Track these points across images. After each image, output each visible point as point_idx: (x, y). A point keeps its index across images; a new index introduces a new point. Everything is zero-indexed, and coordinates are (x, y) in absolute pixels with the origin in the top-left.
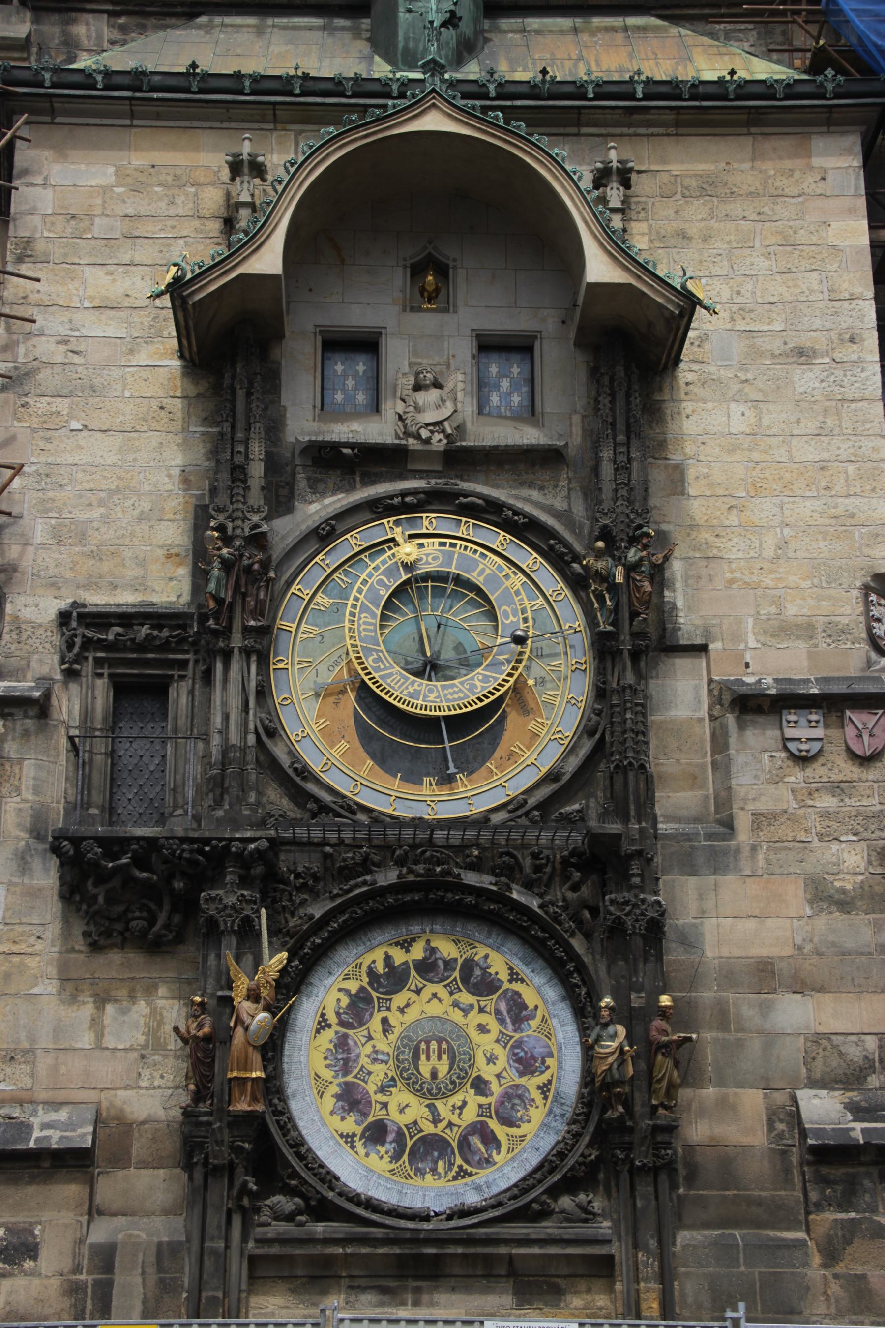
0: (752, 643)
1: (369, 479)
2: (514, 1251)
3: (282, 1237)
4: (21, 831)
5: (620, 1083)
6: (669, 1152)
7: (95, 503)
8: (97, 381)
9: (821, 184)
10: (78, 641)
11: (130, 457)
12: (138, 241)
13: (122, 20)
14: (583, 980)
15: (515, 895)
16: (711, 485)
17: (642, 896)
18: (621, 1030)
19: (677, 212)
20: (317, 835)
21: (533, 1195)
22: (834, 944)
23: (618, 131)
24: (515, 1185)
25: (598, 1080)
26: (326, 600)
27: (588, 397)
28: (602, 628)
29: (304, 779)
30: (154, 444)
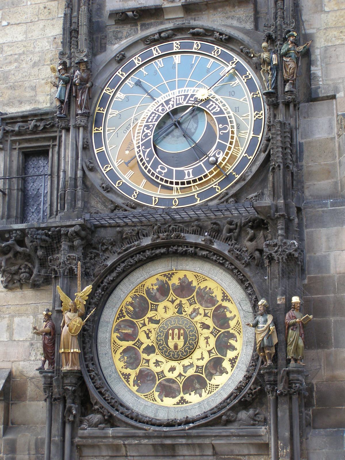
1: (144, 27)
2: (213, 442)
3: (91, 435)
6: (298, 385)
15: (215, 246)
17: (285, 241)
21: (223, 411)
24: (216, 407)
26: (122, 95)
29: (108, 192)
30: (41, 26)
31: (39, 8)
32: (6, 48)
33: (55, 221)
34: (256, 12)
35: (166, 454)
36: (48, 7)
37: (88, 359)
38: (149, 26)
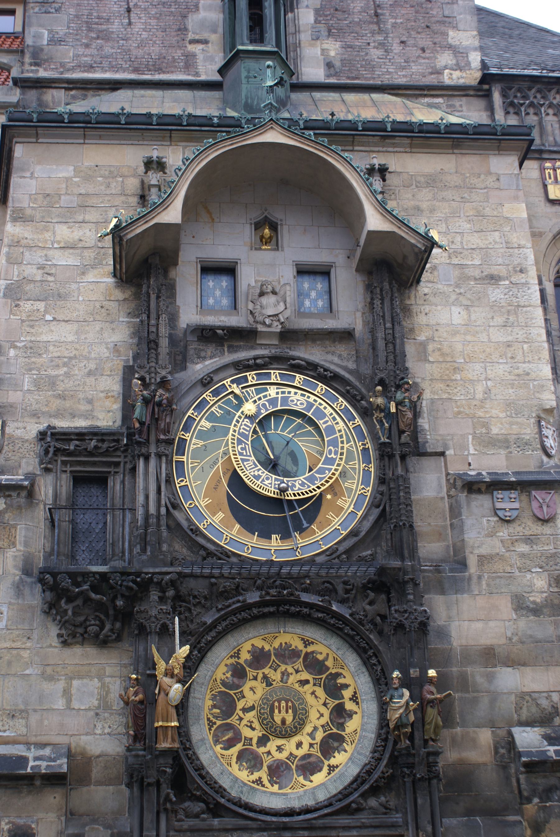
0: (472, 451)
1: (232, 349)
2: (340, 834)
4: (17, 570)
5: (404, 726)
7: (61, 365)
8: (62, 291)
9: (497, 183)
10: (51, 450)
11: (83, 337)
12: (88, 209)
13: (73, 92)
14: (378, 661)
15: (334, 608)
16: (443, 355)
17: (415, 607)
18: (407, 693)
19: (413, 196)
20: (207, 571)
21: (352, 798)
22: (531, 636)
23: (376, 149)
24: (340, 793)
25: (392, 725)
26: (208, 423)
28: (382, 440)
29: (197, 535)
30: (98, 328)
31: (95, 307)
32: (51, 348)
34: (356, 353)
37: (183, 734)
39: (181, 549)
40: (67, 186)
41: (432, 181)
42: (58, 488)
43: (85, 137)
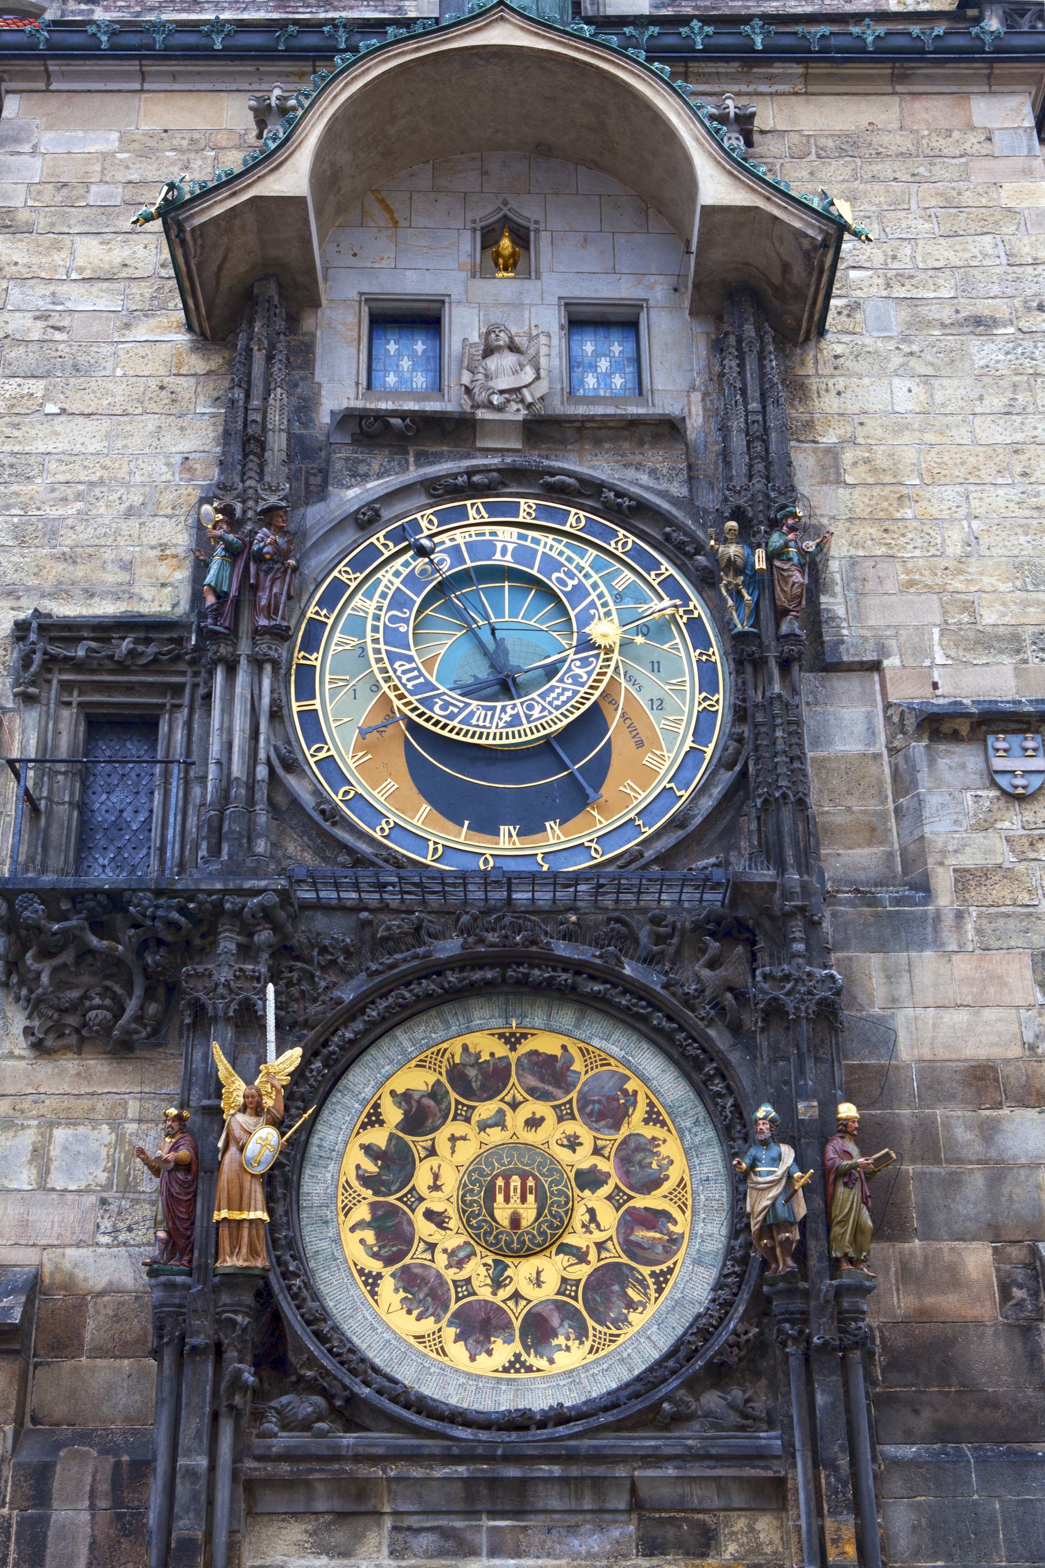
0: (940, 659)
2: (636, 1473)
7: (71, 497)
8: (82, 359)
9: (987, 145)
10: (37, 658)
11: (119, 444)
14: (728, 1087)
15: (628, 971)
16: (874, 471)
17: (808, 969)
19: (812, 174)
24: (638, 1379)
27: (710, 372)
29: (334, 824)
30: (151, 427)
32: (53, 466)
33: (207, 878)
34: (690, 467)
35: (499, 1507)
36: (172, 387)
38: (438, 458)
39: (298, 852)
40: (104, 168)
41: (849, 146)
42: (50, 734)
43: (143, 76)
